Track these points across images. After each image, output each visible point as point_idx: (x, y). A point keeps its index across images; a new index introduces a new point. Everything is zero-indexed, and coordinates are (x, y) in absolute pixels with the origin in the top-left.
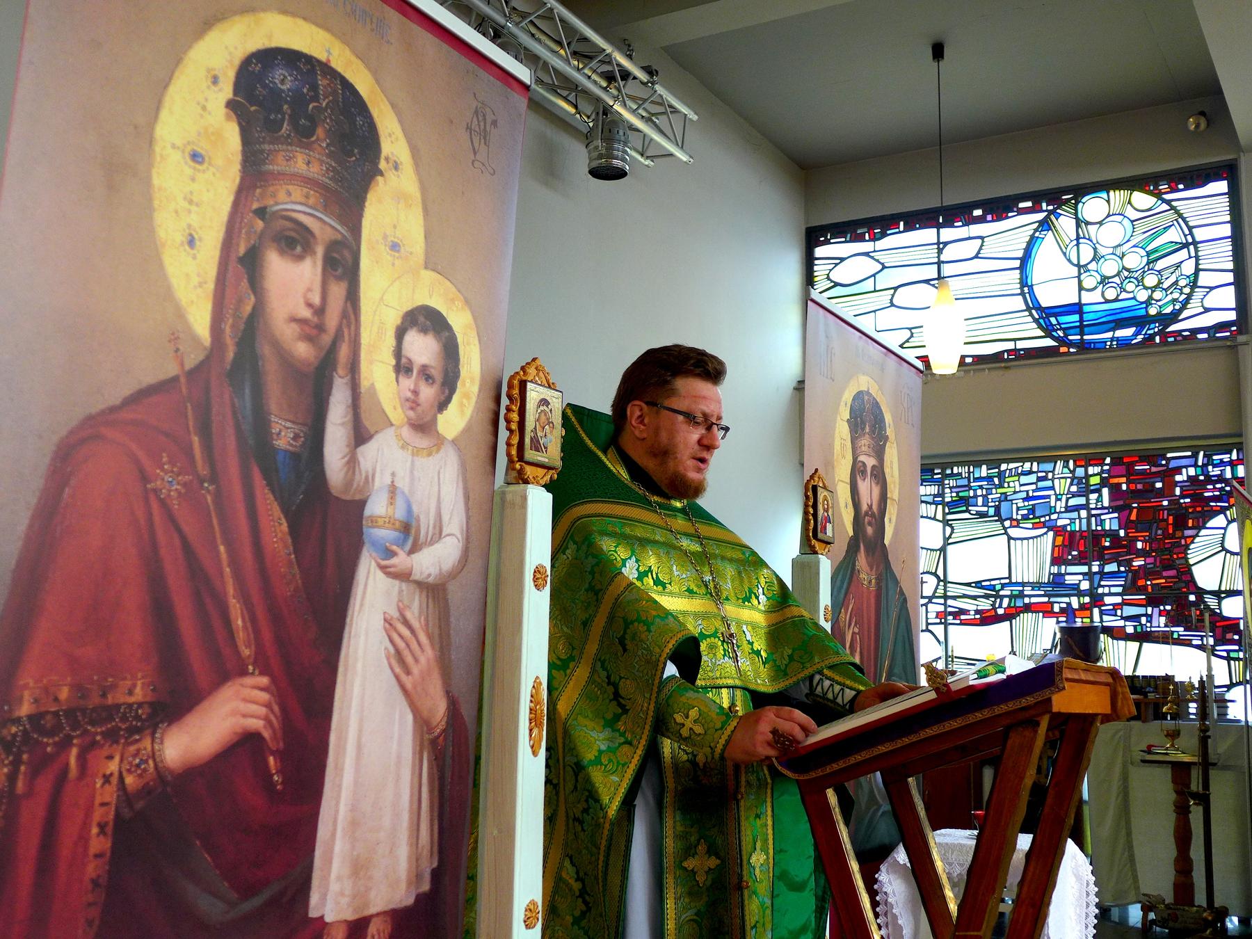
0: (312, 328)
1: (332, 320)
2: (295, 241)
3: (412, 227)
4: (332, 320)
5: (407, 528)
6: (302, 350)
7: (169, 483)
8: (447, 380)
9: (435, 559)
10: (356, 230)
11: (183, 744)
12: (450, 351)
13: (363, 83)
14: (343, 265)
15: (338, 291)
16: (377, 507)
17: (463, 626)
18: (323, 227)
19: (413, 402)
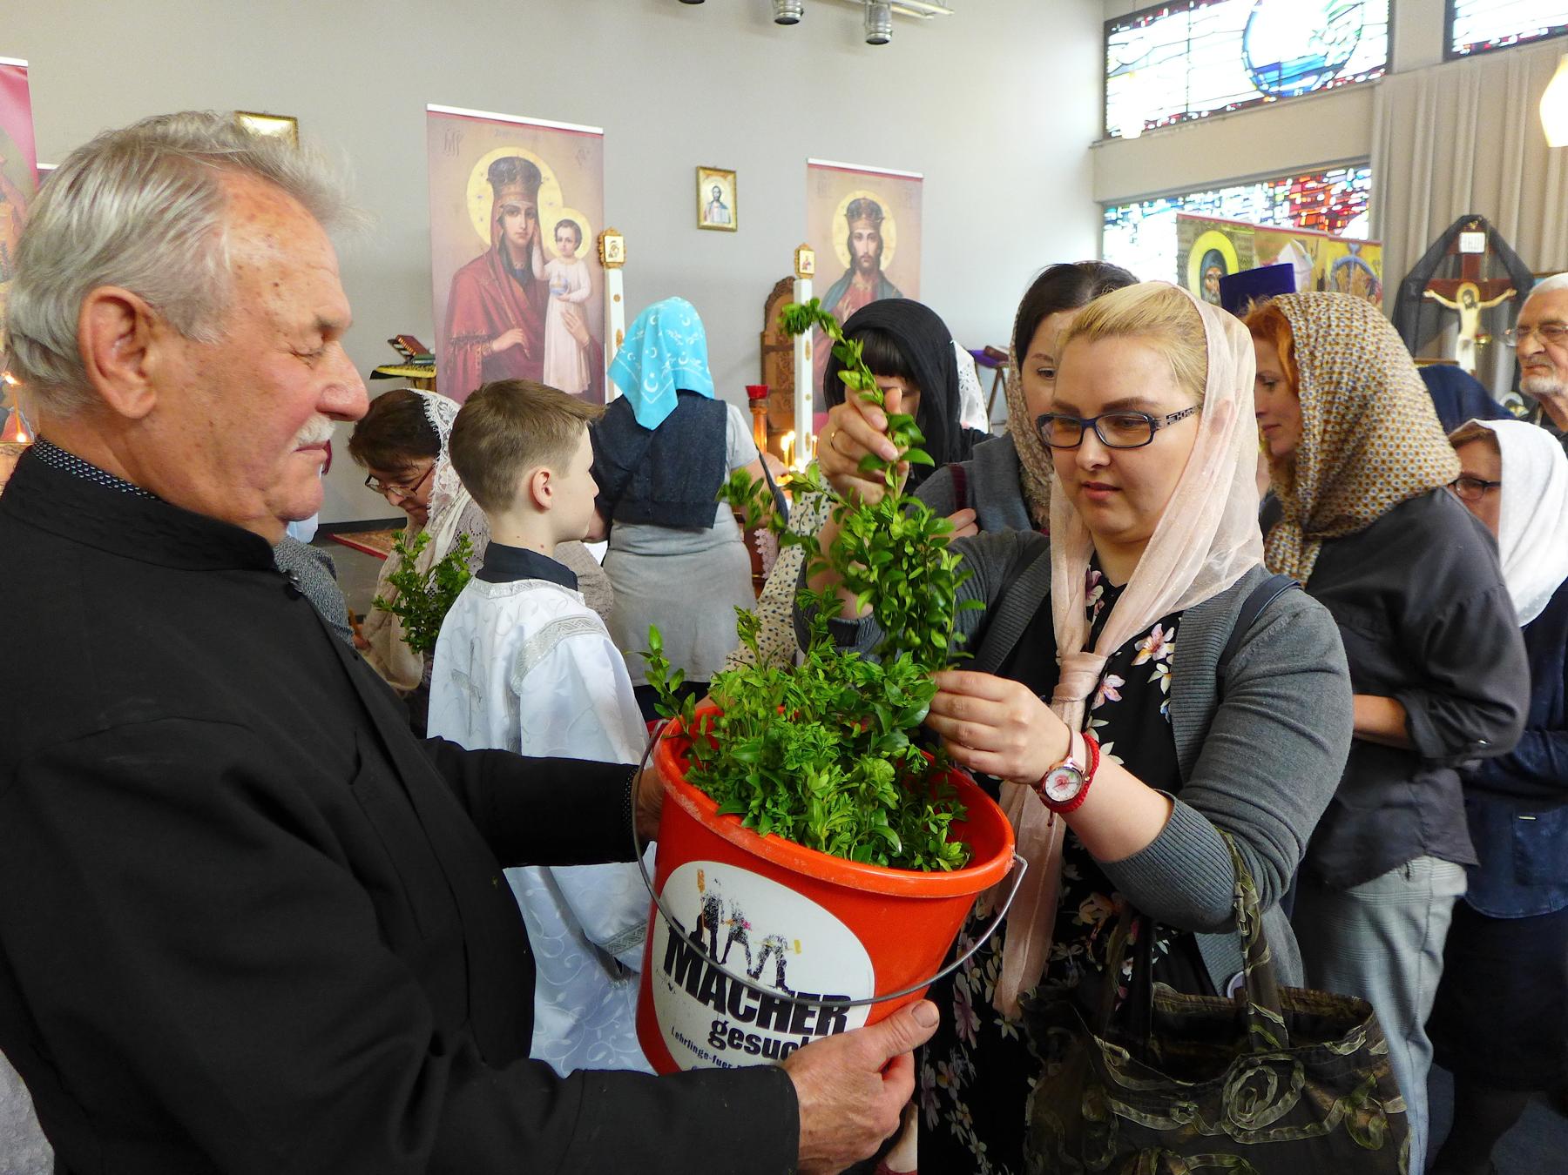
0: (524, 234)
1: (530, 231)
2: (514, 211)
3: (557, 197)
4: (530, 231)
5: (566, 287)
6: (521, 242)
7: (485, 282)
8: (578, 239)
9: (582, 293)
10: (536, 203)
11: (499, 345)
12: (578, 232)
13: (531, 157)
14: (532, 214)
15: (531, 223)
16: (554, 281)
17: (593, 314)
18: (523, 205)
19: (564, 249)
